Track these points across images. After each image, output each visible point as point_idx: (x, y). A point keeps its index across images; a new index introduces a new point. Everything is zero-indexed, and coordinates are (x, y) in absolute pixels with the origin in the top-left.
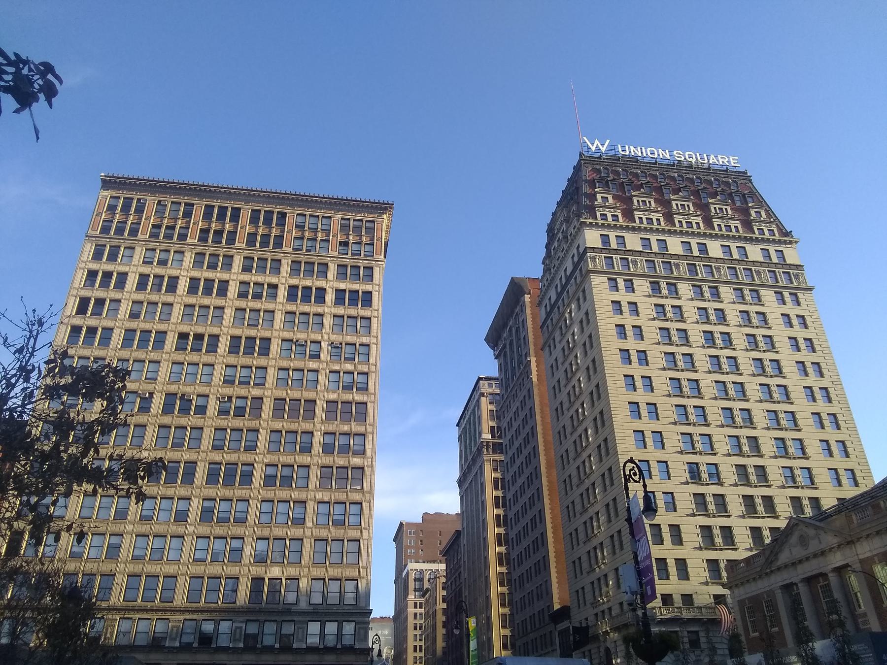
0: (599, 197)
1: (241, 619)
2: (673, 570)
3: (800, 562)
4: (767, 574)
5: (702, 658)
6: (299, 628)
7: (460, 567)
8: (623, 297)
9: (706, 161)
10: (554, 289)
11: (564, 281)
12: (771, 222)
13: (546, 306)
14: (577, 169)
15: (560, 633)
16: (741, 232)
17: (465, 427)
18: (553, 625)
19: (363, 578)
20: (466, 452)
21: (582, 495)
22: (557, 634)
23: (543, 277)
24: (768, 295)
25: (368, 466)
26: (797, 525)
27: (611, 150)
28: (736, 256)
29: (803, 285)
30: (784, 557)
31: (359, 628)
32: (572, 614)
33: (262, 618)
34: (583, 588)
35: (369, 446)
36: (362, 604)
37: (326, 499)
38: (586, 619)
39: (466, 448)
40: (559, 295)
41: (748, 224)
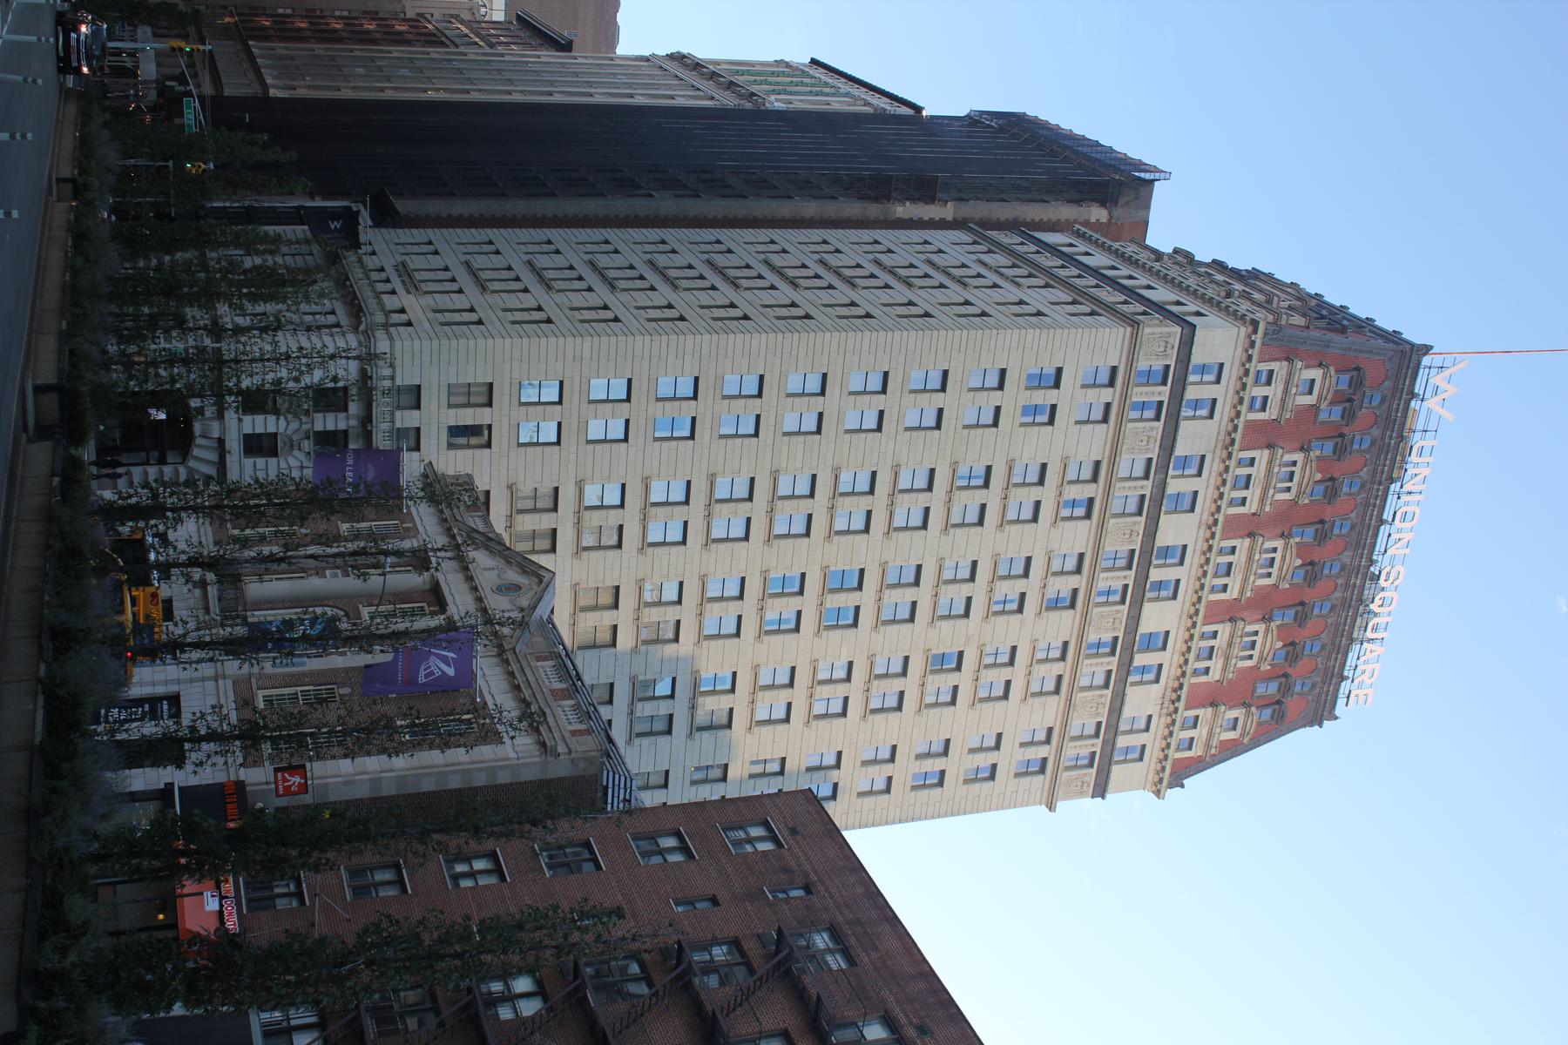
0: (1316, 374)
2: (468, 417)
3: (470, 579)
4: (449, 529)
5: (296, 453)
7: (491, 46)
8: (1072, 399)
9: (1369, 634)
10: (1110, 263)
11: (1124, 282)
12: (1208, 746)
13: (1071, 245)
16: (1194, 680)
17: (808, 76)
20: (748, 73)
21: (632, 267)
23: (1148, 248)
24: (1048, 712)
26: (541, 581)
27: (1428, 419)
28: (1140, 660)
29: (1060, 793)
30: (480, 559)
32: (384, 230)
38: (374, 253)
39: (759, 74)
40: (1095, 272)
41: (1213, 698)
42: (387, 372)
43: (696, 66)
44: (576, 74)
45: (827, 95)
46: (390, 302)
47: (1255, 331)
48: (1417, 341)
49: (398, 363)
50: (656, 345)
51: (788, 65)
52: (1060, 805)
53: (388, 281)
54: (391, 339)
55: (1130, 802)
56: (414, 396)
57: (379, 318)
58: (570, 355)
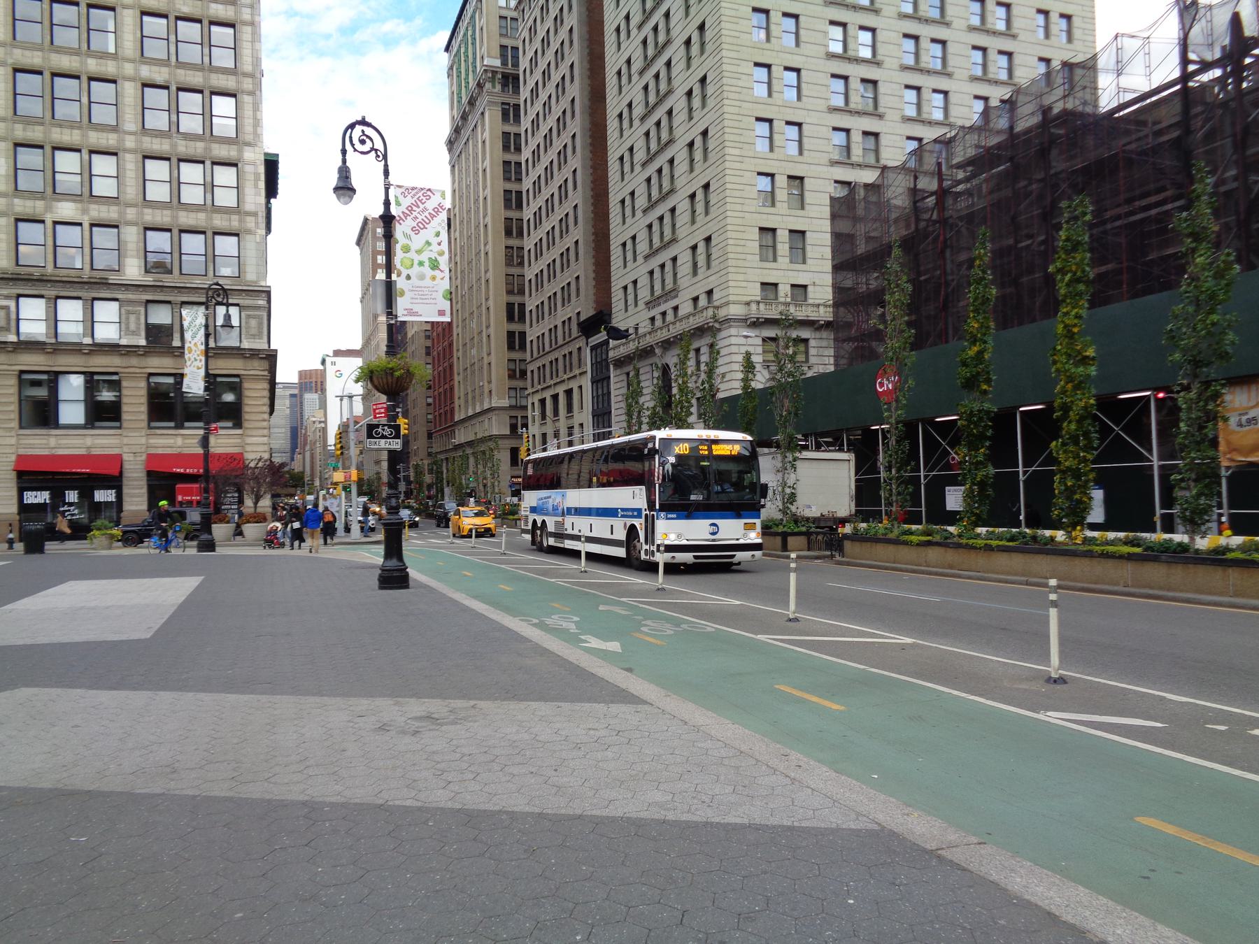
1: (5, 292)
2: (783, 247)
6: (129, 313)
15: (593, 349)
17: (459, 51)
19: (249, 232)
20: (459, 93)
25: (245, 23)
31: (249, 317)
33: (52, 293)
34: (635, 282)
36: (250, 276)
37: (160, 78)
39: (460, 86)
42: (754, 306)
43: (457, 131)
44: (469, 211)
45: (474, 31)
46: (686, 308)
49: (749, 299)
50: (732, 96)
51: (451, 68)
53: (664, 314)
54: (727, 303)
56: (770, 287)
57: (710, 312)
58: (738, 165)
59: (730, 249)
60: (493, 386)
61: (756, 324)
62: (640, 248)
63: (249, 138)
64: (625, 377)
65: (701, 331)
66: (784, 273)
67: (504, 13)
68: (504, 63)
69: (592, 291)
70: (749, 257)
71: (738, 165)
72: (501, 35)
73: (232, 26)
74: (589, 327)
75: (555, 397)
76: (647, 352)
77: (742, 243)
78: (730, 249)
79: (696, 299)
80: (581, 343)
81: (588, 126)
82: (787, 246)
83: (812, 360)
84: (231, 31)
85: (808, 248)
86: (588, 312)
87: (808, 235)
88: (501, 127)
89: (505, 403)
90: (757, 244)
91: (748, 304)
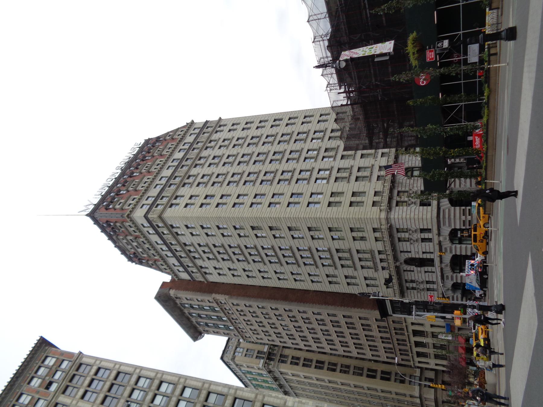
14: (96, 222)
18: (388, 317)
22: (394, 315)
25: (235, 393)
35: (220, 389)
42: (382, 208)
47: (128, 215)
48: (88, 219)
50: (297, 215)
52: (217, 119)
54: (380, 219)
55: (200, 119)
56: (374, 204)
58: (324, 213)
59: (357, 217)
60: (408, 393)
61: (390, 208)
62: (351, 274)
63: (282, 402)
64: (409, 291)
65: (391, 236)
66: (369, 198)
67: (244, 354)
68: (263, 358)
69: (367, 311)
70: (361, 210)
71: (324, 213)
72: (252, 357)
73: (235, 399)
74: (384, 314)
75: (417, 344)
76: (397, 268)
77: (355, 213)
78: (357, 217)
79: (377, 240)
80: (390, 319)
81: (296, 303)
82: (358, 198)
83: (407, 189)
84: (237, 400)
85: (360, 190)
86: (377, 314)
87: (354, 191)
88: (288, 365)
89: (417, 388)
90: (356, 208)
91: (381, 210)
